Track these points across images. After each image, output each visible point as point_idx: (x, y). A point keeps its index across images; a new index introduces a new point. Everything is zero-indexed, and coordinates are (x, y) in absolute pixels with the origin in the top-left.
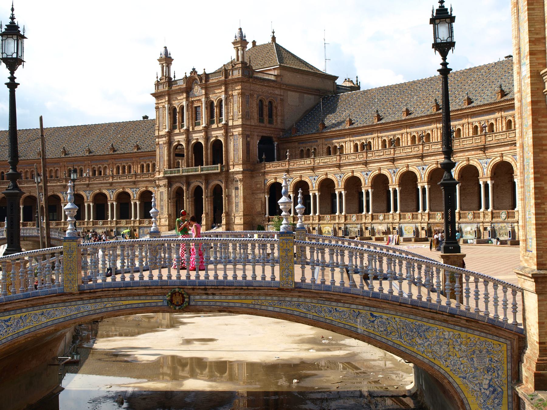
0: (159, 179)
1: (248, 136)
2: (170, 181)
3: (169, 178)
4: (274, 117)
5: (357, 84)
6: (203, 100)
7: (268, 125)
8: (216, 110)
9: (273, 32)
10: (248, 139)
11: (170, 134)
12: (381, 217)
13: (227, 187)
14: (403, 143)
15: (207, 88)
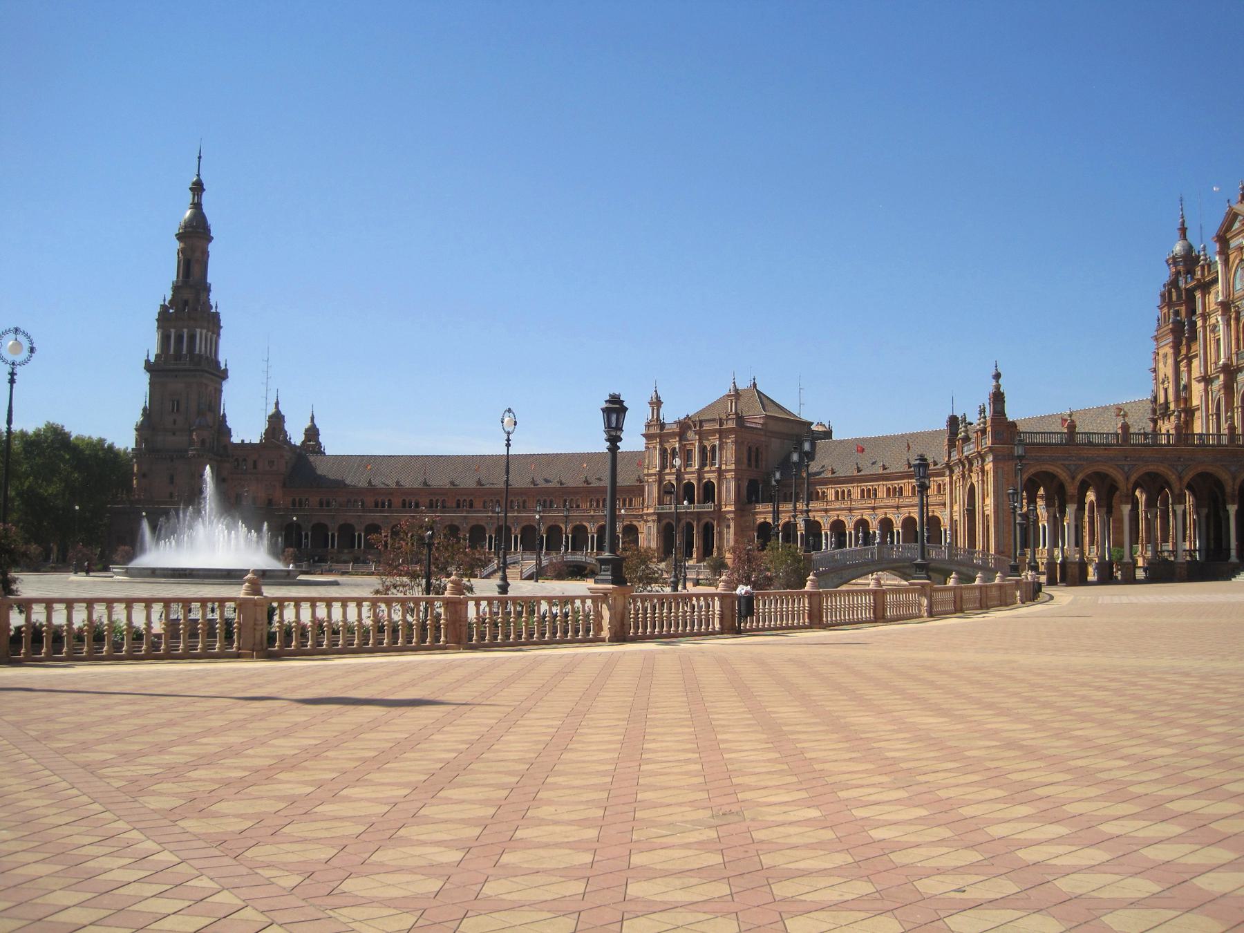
0: (647, 514)
2: (660, 517)
3: (659, 515)
11: (661, 474)
13: (718, 525)
14: (879, 495)
15: (702, 436)
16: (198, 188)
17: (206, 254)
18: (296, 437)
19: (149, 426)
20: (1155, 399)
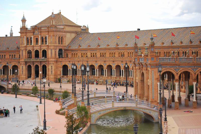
1: (55, 49)
4: (63, 42)
5: (88, 28)
6: (40, 36)
7: (61, 45)
8: (44, 40)
9: (60, 10)
10: (56, 50)
12: (101, 78)
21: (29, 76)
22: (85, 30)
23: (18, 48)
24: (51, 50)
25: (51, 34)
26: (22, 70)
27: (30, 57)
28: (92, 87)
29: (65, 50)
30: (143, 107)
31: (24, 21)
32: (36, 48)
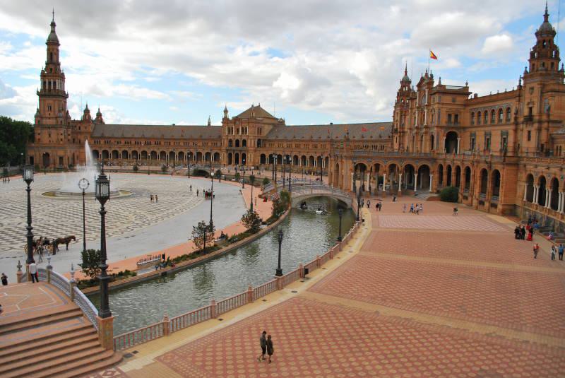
2: (227, 150)
16: (53, 25)
17: (58, 50)
18: (94, 116)
19: (39, 116)
20: (393, 126)
21: (230, 163)
22: (282, 122)
23: (220, 137)
24: (251, 139)
25: (251, 125)
26: (224, 157)
27: (231, 145)
28: (294, 176)
29: (263, 140)
30: (337, 194)
31: (226, 111)
32: (237, 137)
